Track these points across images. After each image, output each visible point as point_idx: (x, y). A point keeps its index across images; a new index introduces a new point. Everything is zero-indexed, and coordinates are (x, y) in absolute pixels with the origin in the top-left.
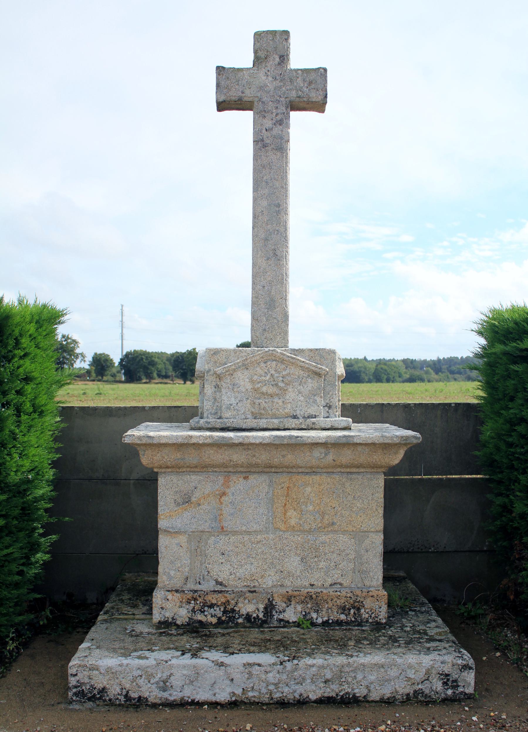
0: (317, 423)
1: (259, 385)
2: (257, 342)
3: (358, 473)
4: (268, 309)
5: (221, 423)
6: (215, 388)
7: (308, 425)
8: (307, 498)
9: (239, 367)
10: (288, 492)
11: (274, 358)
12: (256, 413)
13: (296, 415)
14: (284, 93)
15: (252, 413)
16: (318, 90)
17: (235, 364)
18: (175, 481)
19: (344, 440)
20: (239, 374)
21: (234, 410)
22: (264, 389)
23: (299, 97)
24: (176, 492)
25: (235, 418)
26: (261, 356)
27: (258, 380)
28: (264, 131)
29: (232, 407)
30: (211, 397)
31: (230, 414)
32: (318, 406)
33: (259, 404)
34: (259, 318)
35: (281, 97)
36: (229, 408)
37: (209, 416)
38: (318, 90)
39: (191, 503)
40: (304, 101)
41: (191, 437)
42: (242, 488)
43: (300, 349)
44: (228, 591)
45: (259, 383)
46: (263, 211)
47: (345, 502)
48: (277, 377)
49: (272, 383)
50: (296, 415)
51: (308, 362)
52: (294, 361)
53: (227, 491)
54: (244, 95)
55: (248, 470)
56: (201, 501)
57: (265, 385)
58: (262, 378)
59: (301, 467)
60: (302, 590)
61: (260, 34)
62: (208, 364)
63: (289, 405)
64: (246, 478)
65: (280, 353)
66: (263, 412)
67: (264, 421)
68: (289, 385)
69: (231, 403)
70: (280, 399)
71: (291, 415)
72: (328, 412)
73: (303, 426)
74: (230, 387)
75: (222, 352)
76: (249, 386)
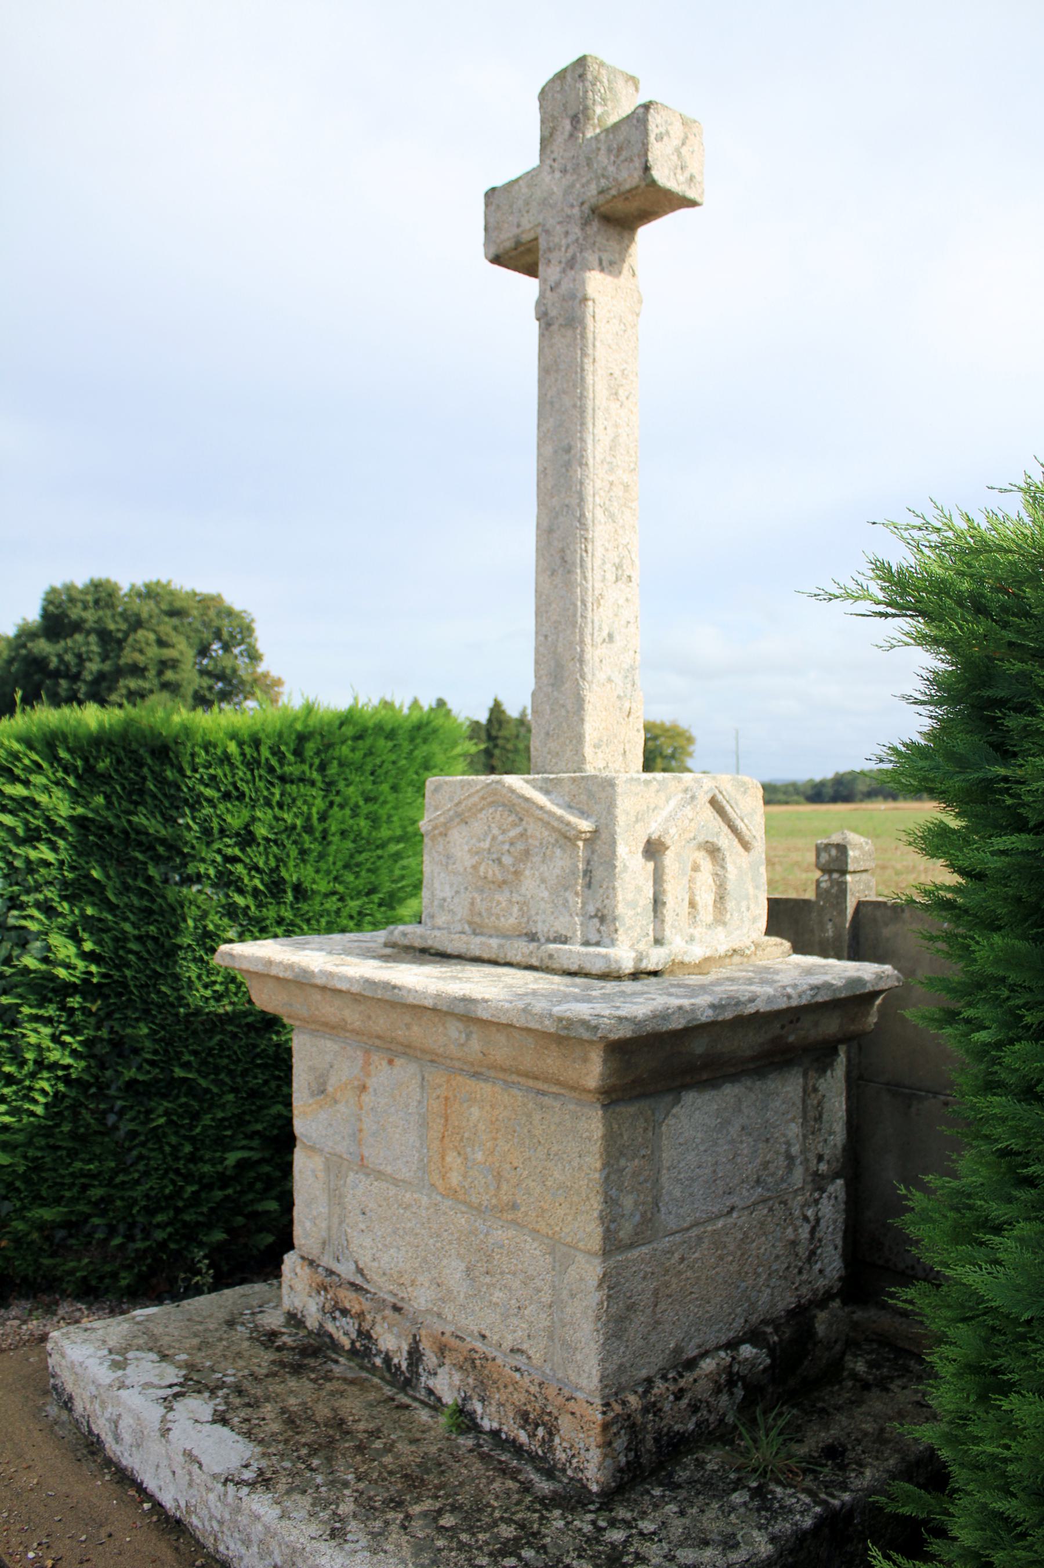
4: (553, 685)
5: (421, 937)
19: (460, 1009)
40: (614, 197)
44: (367, 1292)
55: (395, 1050)
60: (469, 1339)
72: (599, 931)
73: (535, 962)
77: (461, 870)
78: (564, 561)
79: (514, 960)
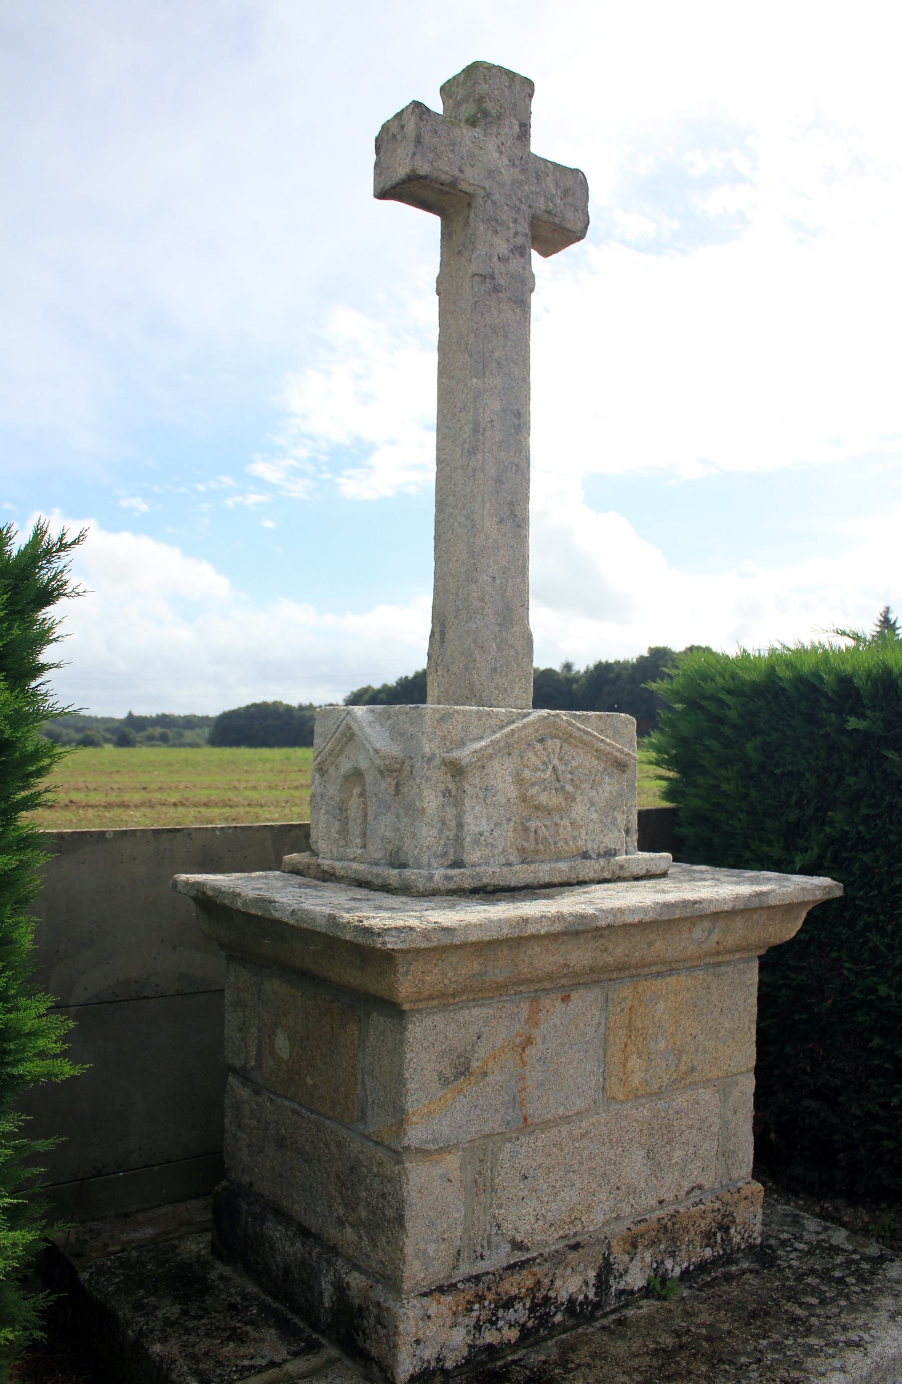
0: (626, 866)
2: (481, 695)
3: (727, 963)
4: (501, 625)
5: (472, 877)
6: (444, 797)
8: (658, 1024)
10: (631, 1019)
11: (554, 731)
13: (587, 851)
14: (527, 197)
16: (577, 210)
18: (441, 1026)
19: (756, 903)
20: (496, 765)
21: (486, 845)
22: (544, 799)
23: (549, 212)
24: (443, 1054)
26: (537, 726)
27: (533, 779)
28: (495, 259)
29: (482, 839)
30: (436, 819)
31: (478, 854)
34: (485, 645)
35: (521, 202)
37: (433, 860)
38: (577, 210)
39: (471, 1074)
41: (526, 921)
42: (559, 1023)
44: (534, 1259)
46: (492, 421)
47: (710, 1024)
48: (563, 772)
53: (535, 1032)
54: (461, 175)
56: (489, 1066)
57: (544, 790)
58: (539, 774)
59: (656, 964)
60: (648, 1216)
61: (491, 68)
62: (430, 741)
64: (566, 999)
65: (567, 721)
67: (546, 867)
69: (481, 829)
73: (607, 875)
75: (456, 715)
76: (513, 792)
77: (503, 801)
78: (513, 515)
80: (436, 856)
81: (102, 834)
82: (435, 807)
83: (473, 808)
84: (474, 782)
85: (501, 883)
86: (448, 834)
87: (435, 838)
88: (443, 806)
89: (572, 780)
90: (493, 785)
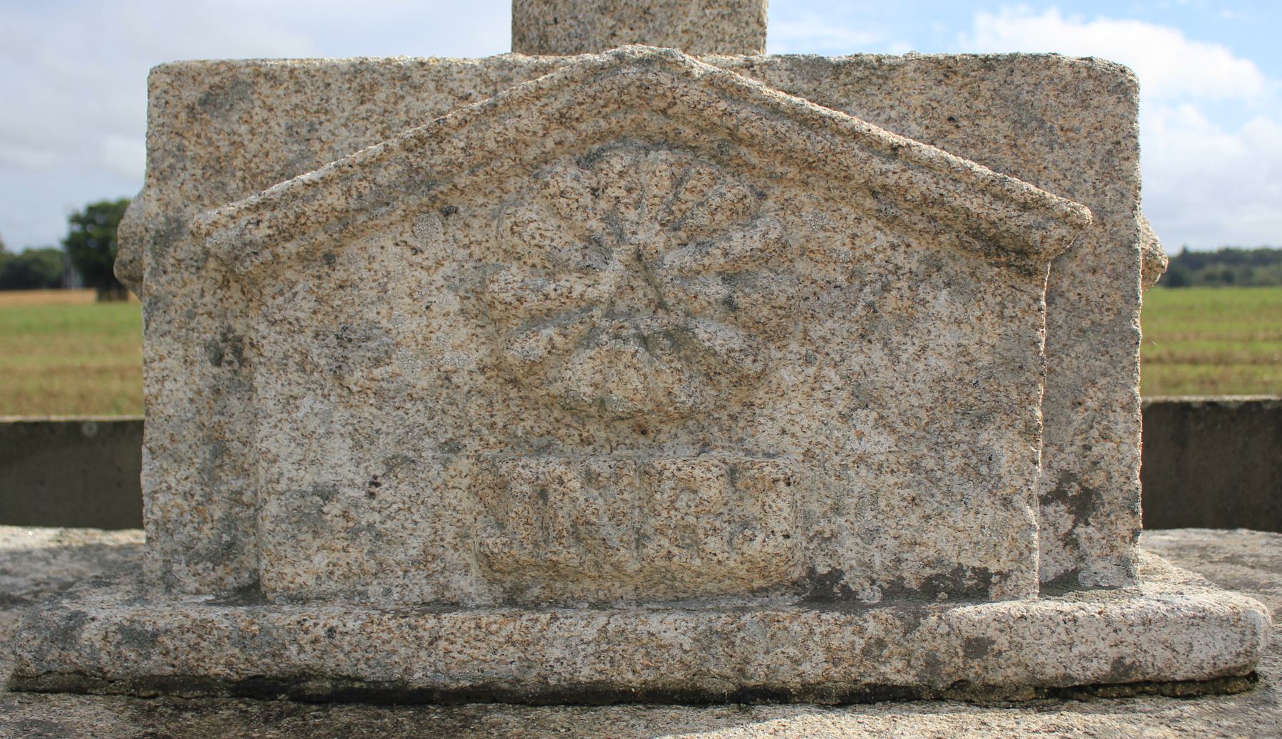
0: (1002, 642)
1: (536, 345)
5: (243, 640)
6: (218, 361)
7: (932, 663)
9: (384, 198)
11: (655, 124)
12: (519, 567)
13: (836, 575)
15: (487, 560)
17: (344, 175)
20: (382, 253)
21: (354, 533)
22: (581, 373)
25: (355, 596)
26: (556, 105)
27: (533, 301)
29: (333, 509)
30: (190, 434)
31: (321, 561)
32: (1007, 502)
33: (543, 494)
36: (312, 510)
37: (180, 569)
43: (858, 61)
45: (535, 321)
48: (687, 275)
49: (648, 323)
50: (836, 575)
51: (931, 151)
52: (818, 144)
57: (589, 340)
58: (565, 281)
63: (782, 503)
65: (711, 80)
66: (569, 555)
68: (777, 336)
69: (327, 477)
70: (705, 446)
71: (797, 573)
72: (1070, 541)
73: (894, 671)
74: (318, 354)
75: (265, 88)
76: (463, 350)
79: (788, 677)
80: (191, 554)
81: (74, 428)
82: (184, 394)
83: (290, 402)
84: (290, 314)
85: (364, 670)
86: (237, 484)
87: (188, 495)
88: (217, 391)
89: (729, 303)
90: (374, 325)
